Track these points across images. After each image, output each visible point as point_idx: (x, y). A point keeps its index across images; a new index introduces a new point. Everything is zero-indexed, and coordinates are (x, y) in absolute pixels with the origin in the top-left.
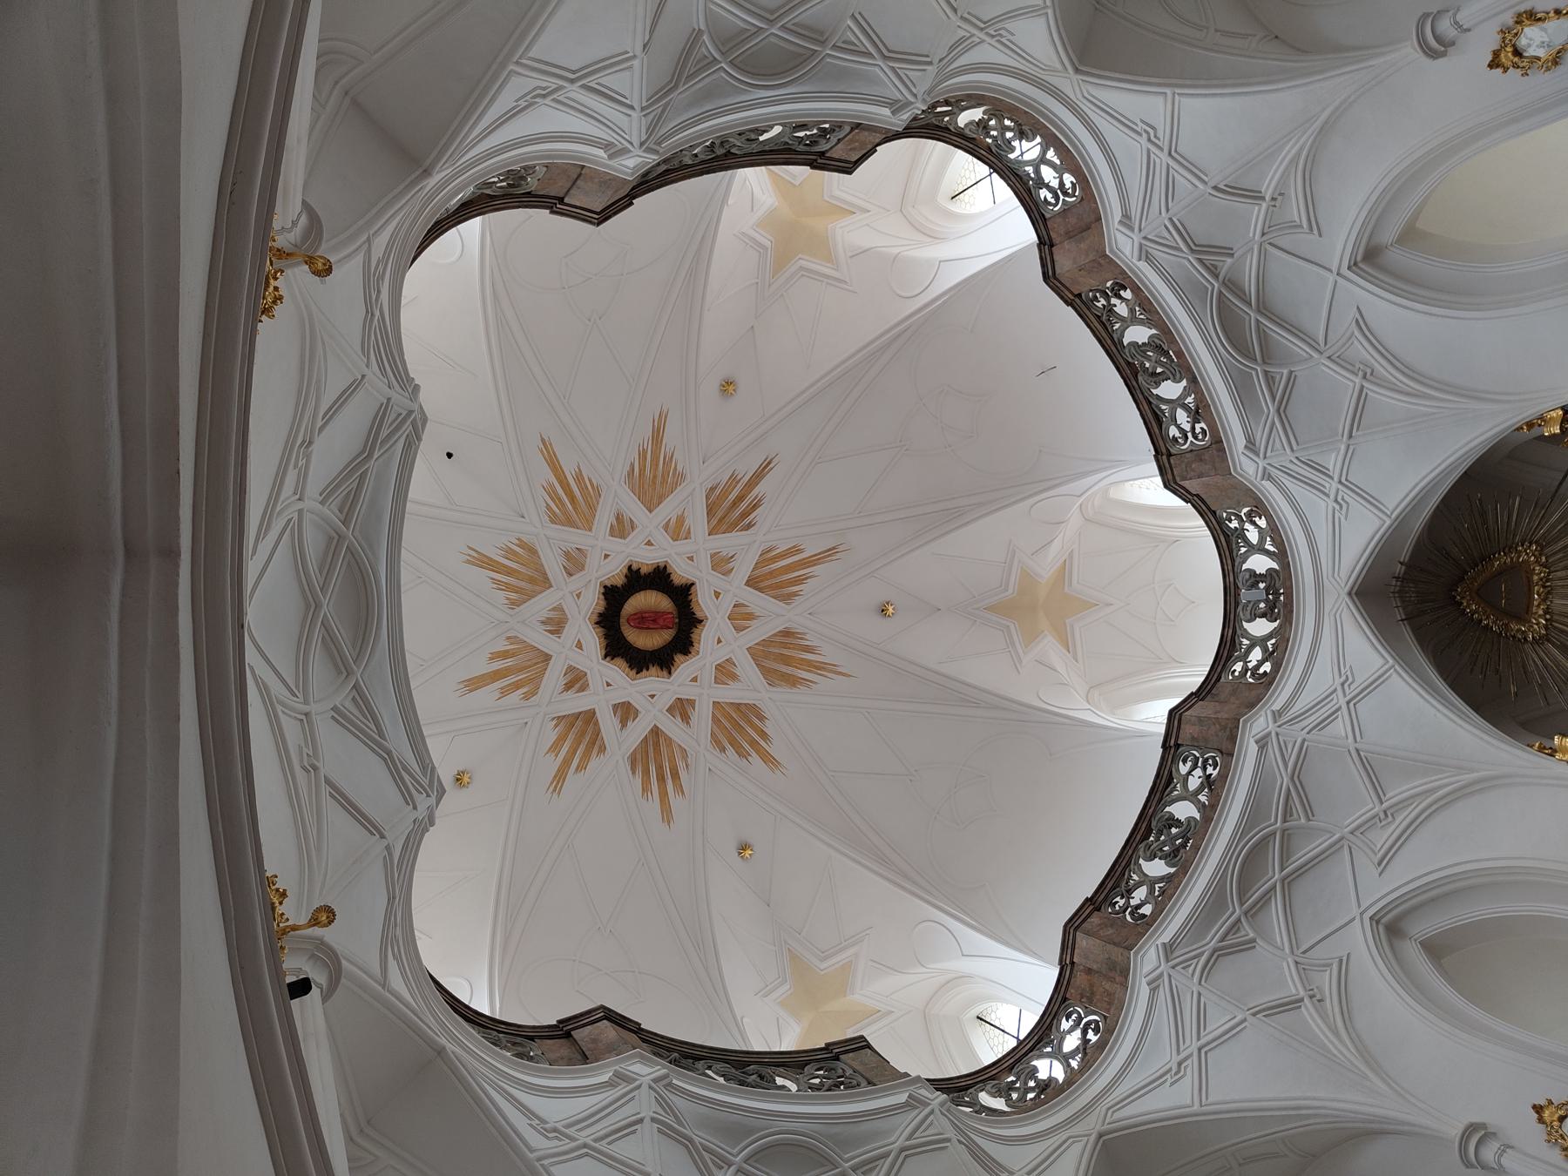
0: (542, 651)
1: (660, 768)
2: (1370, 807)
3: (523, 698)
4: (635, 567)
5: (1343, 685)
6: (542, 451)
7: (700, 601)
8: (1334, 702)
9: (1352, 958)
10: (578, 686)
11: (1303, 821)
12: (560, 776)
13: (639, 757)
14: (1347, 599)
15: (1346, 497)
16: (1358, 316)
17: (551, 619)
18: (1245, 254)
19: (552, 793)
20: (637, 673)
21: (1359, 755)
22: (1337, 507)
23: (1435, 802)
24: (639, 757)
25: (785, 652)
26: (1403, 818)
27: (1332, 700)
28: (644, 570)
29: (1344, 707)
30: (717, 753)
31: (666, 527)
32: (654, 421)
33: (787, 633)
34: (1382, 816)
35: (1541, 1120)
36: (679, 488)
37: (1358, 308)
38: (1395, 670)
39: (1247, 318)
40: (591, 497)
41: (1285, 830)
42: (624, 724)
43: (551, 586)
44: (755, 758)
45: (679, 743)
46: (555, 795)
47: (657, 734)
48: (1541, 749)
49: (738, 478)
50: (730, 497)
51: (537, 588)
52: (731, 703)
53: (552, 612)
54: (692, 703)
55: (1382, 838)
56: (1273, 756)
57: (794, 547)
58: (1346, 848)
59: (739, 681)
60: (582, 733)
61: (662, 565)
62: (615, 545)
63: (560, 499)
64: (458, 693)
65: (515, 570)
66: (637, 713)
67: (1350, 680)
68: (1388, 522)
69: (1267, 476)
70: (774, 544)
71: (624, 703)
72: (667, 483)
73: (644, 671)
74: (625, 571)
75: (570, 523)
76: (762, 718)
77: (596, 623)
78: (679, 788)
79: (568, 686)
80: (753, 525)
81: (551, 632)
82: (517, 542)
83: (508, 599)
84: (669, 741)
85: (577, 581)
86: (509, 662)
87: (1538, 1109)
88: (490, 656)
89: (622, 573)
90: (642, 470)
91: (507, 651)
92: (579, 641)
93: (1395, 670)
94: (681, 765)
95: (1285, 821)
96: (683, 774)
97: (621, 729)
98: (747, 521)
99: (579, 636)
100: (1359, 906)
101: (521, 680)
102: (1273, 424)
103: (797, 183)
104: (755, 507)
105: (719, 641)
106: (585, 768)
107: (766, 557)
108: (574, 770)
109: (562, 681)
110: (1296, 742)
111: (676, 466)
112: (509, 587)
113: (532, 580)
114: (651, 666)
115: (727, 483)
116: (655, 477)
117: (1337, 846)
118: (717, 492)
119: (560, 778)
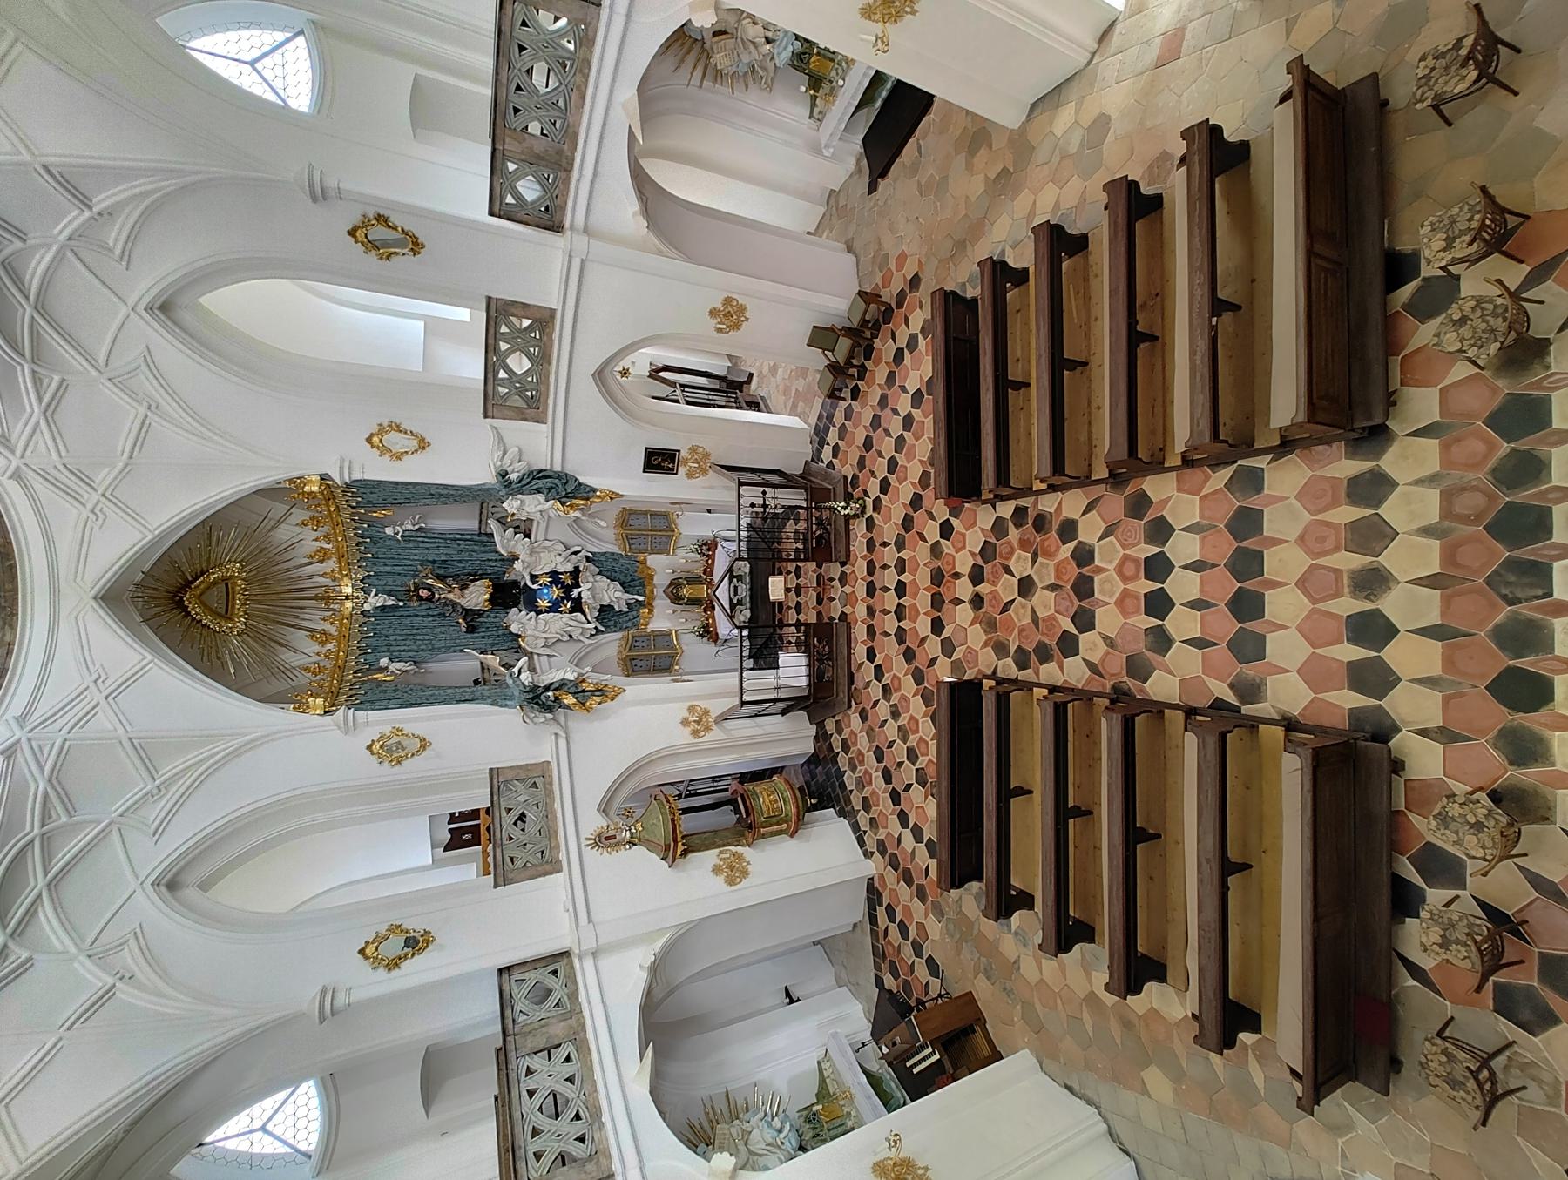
2: (141, 785)
5: (95, 682)
8: (88, 699)
9: (144, 925)
11: (64, 819)
14: (93, 603)
15: (105, 509)
16: (146, 353)
18: (40, 246)
21: (132, 743)
22: (93, 517)
23: (213, 765)
26: (176, 790)
27: (86, 697)
29: (103, 702)
34: (155, 791)
35: (367, 958)
37: (147, 347)
38: (155, 664)
39: (21, 311)
41: (43, 835)
48: (295, 709)
55: (154, 812)
56: (23, 764)
58: (115, 834)
67: (103, 677)
68: (150, 537)
69: (17, 476)
87: (362, 952)
93: (155, 664)
95: (43, 825)
100: (137, 878)
102: (37, 425)
110: (53, 744)
117: (107, 831)
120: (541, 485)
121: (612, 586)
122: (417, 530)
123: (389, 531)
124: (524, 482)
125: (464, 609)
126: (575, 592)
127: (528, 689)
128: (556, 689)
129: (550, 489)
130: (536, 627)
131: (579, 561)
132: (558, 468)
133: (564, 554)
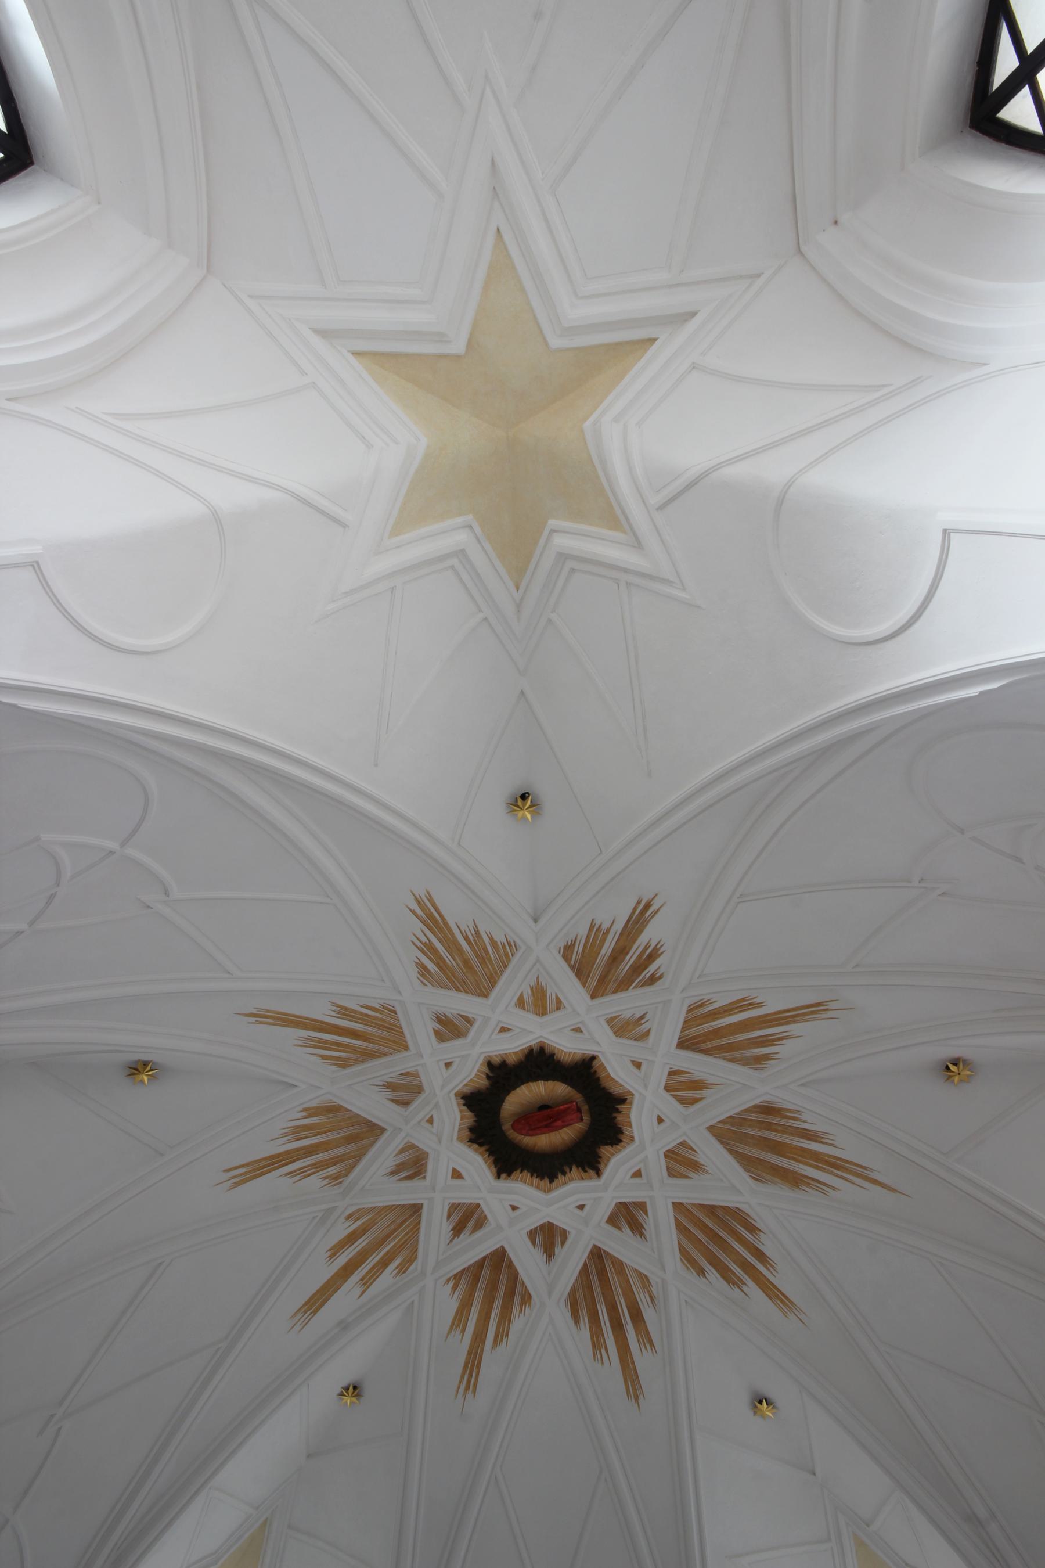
0: (404, 1205)
1: (613, 1309)
3: (398, 1273)
4: (497, 1061)
6: (261, 1023)
7: (612, 1075)
10: (470, 1225)
12: (473, 1361)
13: (580, 1297)
17: (402, 1164)
19: (465, 1394)
20: (550, 1182)
24: (580, 1297)
25: (770, 1135)
28: (512, 1060)
30: (692, 1276)
31: (521, 1003)
32: (414, 912)
33: (767, 1109)
36: (514, 961)
40: (383, 1020)
42: (549, 1252)
43: (383, 1130)
44: (751, 1287)
45: (635, 1266)
46: (470, 1394)
47: (600, 1257)
49: (605, 927)
50: (603, 951)
51: (364, 1142)
52: (700, 1204)
53: (402, 1155)
54: (642, 1206)
57: (743, 1000)
59: (706, 1172)
60: (492, 1287)
61: (536, 1048)
62: (454, 1048)
63: (336, 1044)
64: (298, 1327)
65: (311, 1146)
66: (564, 1234)
70: (707, 998)
71: (542, 1227)
72: (490, 960)
73: (561, 1177)
74: (485, 1069)
75: (368, 1056)
76: (753, 1229)
77: (472, 1141)
78: (646, 1337)
79: (458, 1230)
80: (660, 977)
81: (409, 1178)
82: (304, 1114)
83: (325, 1178)
84: (619, 1266)
85: (419, 1108)
86: (361, 1243)
88: (329, 1253)
89: (483, 1073)
90: (440, 963)
91: (354, 1232)
92: (454, 1171)
94: (642, 1298)
96: (648, 1314)
97: (548, 1261)
98: (647, 973)
99: (452, 1165)
101: (388, 1253)
103: (458, 346)
104: (653, 955)
105: (660, 1120)
106: (507, 1335)
107: (697, 1014)
108: (491, 1343)
109: (447, 1227)
111: (491, 939)
112: (319, 1166)
113: (351, 1139)
114: (567, 1170)
115: (588, 937)
116: (466, 962)
118: (579, 949)
119: (473, 1366)
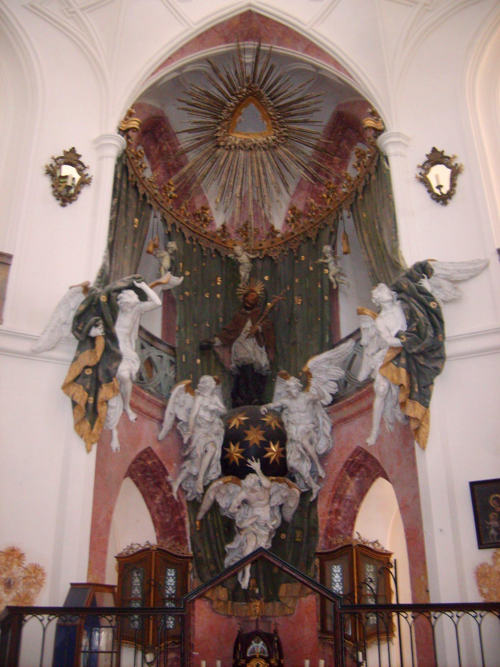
34: (71, 10)
38: (188, 30)
120: (420, 314)
121: (265, 533)
122: (329, 280)
123: (327, 248)
124: (421, 296)
125: (234, 340)
126: (256, 465)
127: (114, 295)
128: (107, 350)
129: (418, 332)
130: (206, 408)
131: (301, 476)
132: (450, 349)
133: (311, 450)
